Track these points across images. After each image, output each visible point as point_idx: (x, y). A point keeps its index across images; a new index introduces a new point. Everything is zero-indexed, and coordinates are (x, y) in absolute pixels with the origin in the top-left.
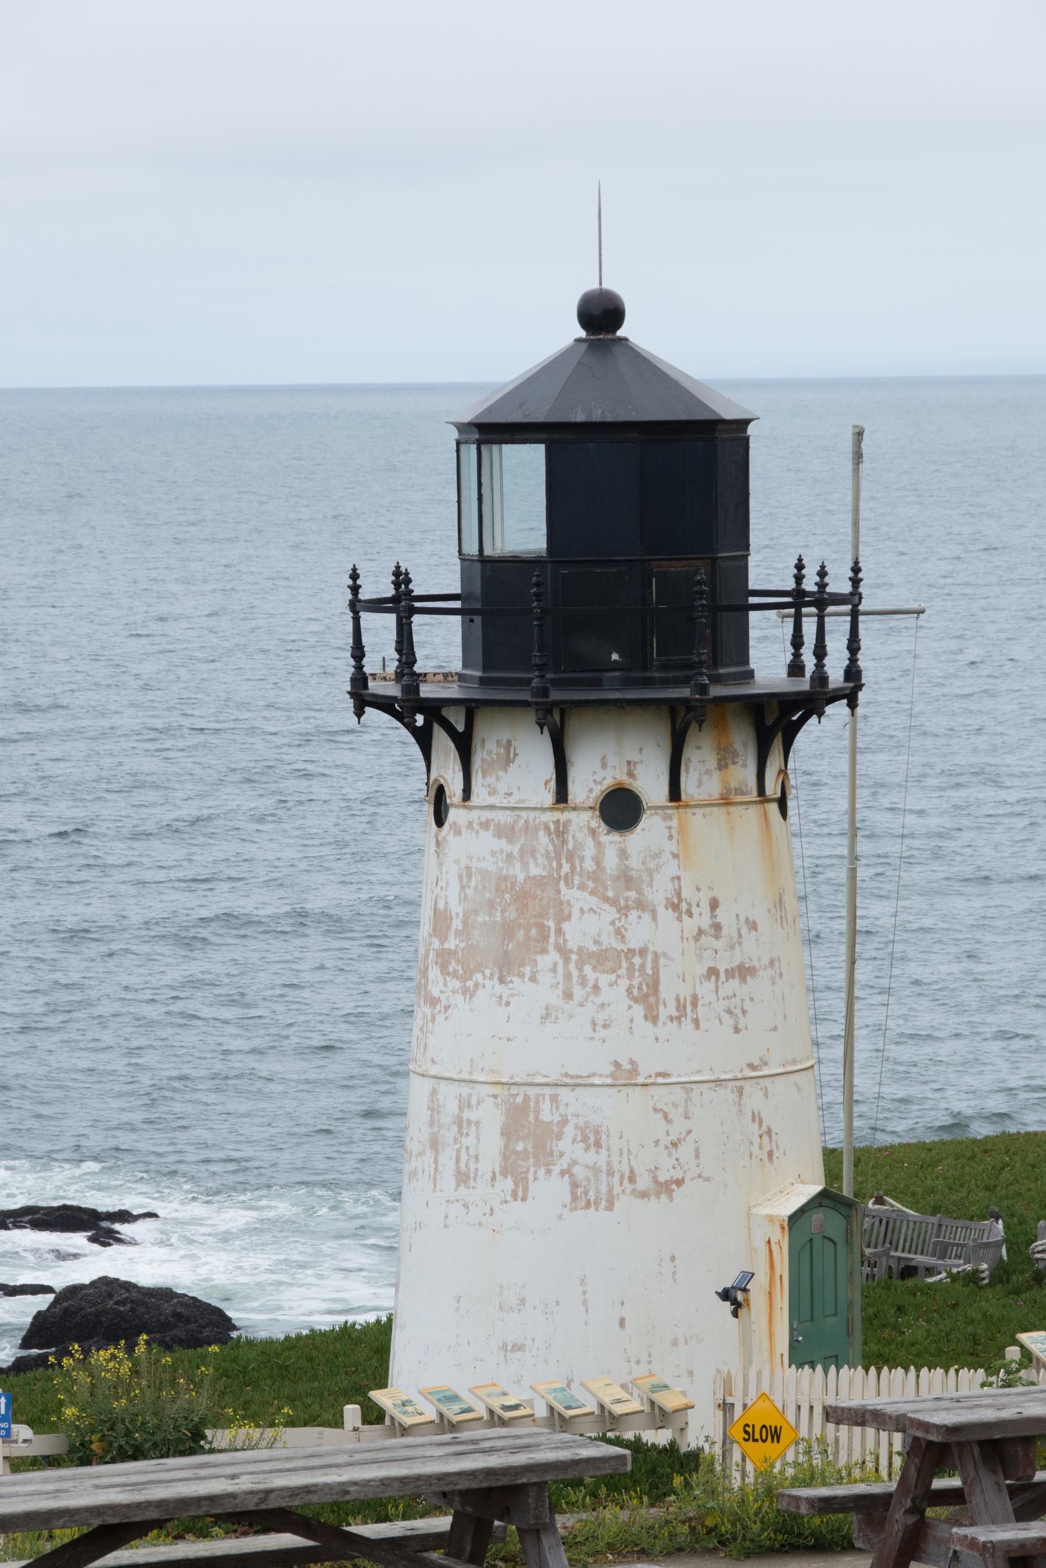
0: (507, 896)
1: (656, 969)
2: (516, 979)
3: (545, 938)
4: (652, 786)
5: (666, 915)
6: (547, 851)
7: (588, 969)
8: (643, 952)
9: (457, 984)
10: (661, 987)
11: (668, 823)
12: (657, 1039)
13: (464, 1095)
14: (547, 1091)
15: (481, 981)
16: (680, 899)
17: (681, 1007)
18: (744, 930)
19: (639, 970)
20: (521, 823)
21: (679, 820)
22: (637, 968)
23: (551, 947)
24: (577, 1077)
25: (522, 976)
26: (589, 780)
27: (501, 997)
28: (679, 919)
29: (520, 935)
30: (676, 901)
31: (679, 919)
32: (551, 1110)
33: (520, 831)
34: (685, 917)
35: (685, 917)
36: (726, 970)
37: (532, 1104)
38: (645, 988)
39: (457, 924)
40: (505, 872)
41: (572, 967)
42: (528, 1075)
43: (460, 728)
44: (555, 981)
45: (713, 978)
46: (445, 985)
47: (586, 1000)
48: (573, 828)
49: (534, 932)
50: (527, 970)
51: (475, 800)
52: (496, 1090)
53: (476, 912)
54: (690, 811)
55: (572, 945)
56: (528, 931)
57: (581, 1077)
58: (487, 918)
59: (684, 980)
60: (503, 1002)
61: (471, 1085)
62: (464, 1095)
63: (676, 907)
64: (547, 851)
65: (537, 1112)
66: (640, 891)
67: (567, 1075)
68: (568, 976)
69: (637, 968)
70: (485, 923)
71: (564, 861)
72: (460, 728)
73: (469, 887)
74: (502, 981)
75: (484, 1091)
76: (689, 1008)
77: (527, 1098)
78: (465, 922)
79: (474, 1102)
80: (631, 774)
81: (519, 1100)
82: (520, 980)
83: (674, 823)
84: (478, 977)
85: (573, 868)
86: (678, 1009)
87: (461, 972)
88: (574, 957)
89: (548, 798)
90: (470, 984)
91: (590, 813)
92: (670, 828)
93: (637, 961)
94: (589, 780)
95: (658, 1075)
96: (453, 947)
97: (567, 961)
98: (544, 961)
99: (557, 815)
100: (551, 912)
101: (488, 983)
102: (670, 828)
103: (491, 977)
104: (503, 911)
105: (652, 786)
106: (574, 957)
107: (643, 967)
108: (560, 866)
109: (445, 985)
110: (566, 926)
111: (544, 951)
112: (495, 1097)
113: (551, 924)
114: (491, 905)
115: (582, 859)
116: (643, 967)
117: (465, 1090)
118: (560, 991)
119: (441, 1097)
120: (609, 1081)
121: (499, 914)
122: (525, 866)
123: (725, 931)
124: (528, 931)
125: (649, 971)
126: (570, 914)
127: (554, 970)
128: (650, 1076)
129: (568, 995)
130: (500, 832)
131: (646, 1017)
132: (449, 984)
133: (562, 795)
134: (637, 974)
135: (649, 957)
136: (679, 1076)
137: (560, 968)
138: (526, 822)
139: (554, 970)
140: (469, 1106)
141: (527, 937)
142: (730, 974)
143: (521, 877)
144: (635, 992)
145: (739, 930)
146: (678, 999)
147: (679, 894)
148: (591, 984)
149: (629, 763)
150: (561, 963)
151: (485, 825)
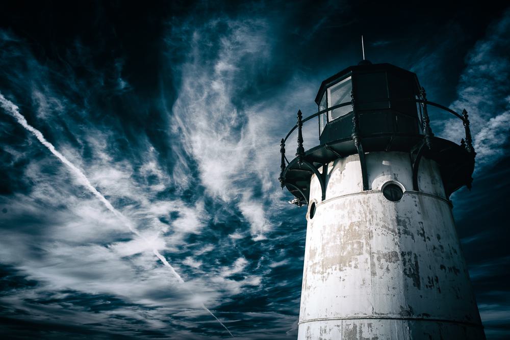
0: (342, 233)
1: (417, 263)
2: (348, 268)
3: (361, 248)
4: (404, 184)
5: (418, 238)
6: (360, 211)
7: (383, 261)
8: (409, 253)
9: (319, 276)
10: (420, 270)
11: (414, 199)
12: (421, 296)
13: (323, 327)
14: (366, 322)
15: (330, 272)
16: (424, 232)
17: (430, 281)
18: (453, 252)
19: (408, 262)
20: (348, 201)
21: (419, 199)
22: (407, 260)
23: (364, 252)
24: (382, 314)
25: (350, 266)
26: (379, 182)
27: (340, 278)
28: (425, 240)
29: (349, 248)
30: (422, 232)
31: (425, 240)
32: (368, 332)
33: (347, 204)
34: (427, 240)
35: (427, 240)
36: (449, 268)
37: (358, 329)
38: (412, 270)
39: (319, 250)
40: (341, 223)
41: (375, 260)
42: (355, 314)
43: (321, 172)
44: (367, 267)
45: (444, 270)
46: (314, 279)
47: (383, 275)
48: (371, 200)
49: (355, 246)
50: (353, 263)
51: (327, 198)
52: (339, 322)
53: (328, 243)
54: (423, 197)
55: (374, 250)
56: (353, 244)
57: (383, 314)
58: (333, 244)
59: (430, 269)
60: (342, 280)
61: (326, 322)
62: (323, 327)
63: (423, 235)
64: (360, 211)
65: (361, 332)
66: (405, 226)
67: (376, 313)
68: (373, 265)
69: (407, 260)
70: (332, 247)
71: (368, 214)
72: (321, 172)
73: (325, 234)
74: (340, 270)
75: (331, 324)
76: (435, 283)
77: (355, 327)
78: (323, 249)
79: (328, 330)
80: (396, 179)
81: (351, 327)
82: (349, 268)
83: (417, 200)
84: (329, 270)
85: (372, 217)
86: (429, 282)
87: (321, 270)
88: (376, 256)
89: (360, 188)
90: (325, 275)
91: (379, 194)
92: (415, 201)
93: (407, 257)
94: (379, 182)
95: (424, 314)
96: (317, 262)
97: (372, 257)
98: (361, 259)
99: (364, 195)
100: (363, 236)
101: (334, 272)
102: (415, 201)
103: (335, 270)
104: (340, 239)
105: (404, 184)
106: (376, 256)
107: (410, 260)
108: (366, 216)
109: (314, 279)
110: (371, 242)
111: (360, 254)
112: (338, 326)
113: (364, 241)
114: (335, 237)
115: (376, 212)
116: (410, 260)
117: (323, 324)
118: (369, 272)
119: (311, 330)
120: (399, 316)
121: (339, 240)
122: (350, 218)
123: (445, 250)
124: (353, 244)
125: (413, 262)
126: (372, 236)
127: (366, 262)
128: (420, 315)
129: (374, 274)
130: (338, 208)
131: (414, 284)
132: (316, 278)
133: (366, 186)
134: (407, 264)
135: (413, 256)
136: (434, 316)
137: (369, 261)
138: (350, 201)
139: (366, 262)
140: (325, 332)
141: (353, 249)
142: (450, 269)
143: (348, 224)
144: (408, 273)
145: (450, 251)
146: (429, 278)
147: (423, 230)
148: (385, 267)
149: (395, 174)
150: (369, 258)
151: (332, 207)
